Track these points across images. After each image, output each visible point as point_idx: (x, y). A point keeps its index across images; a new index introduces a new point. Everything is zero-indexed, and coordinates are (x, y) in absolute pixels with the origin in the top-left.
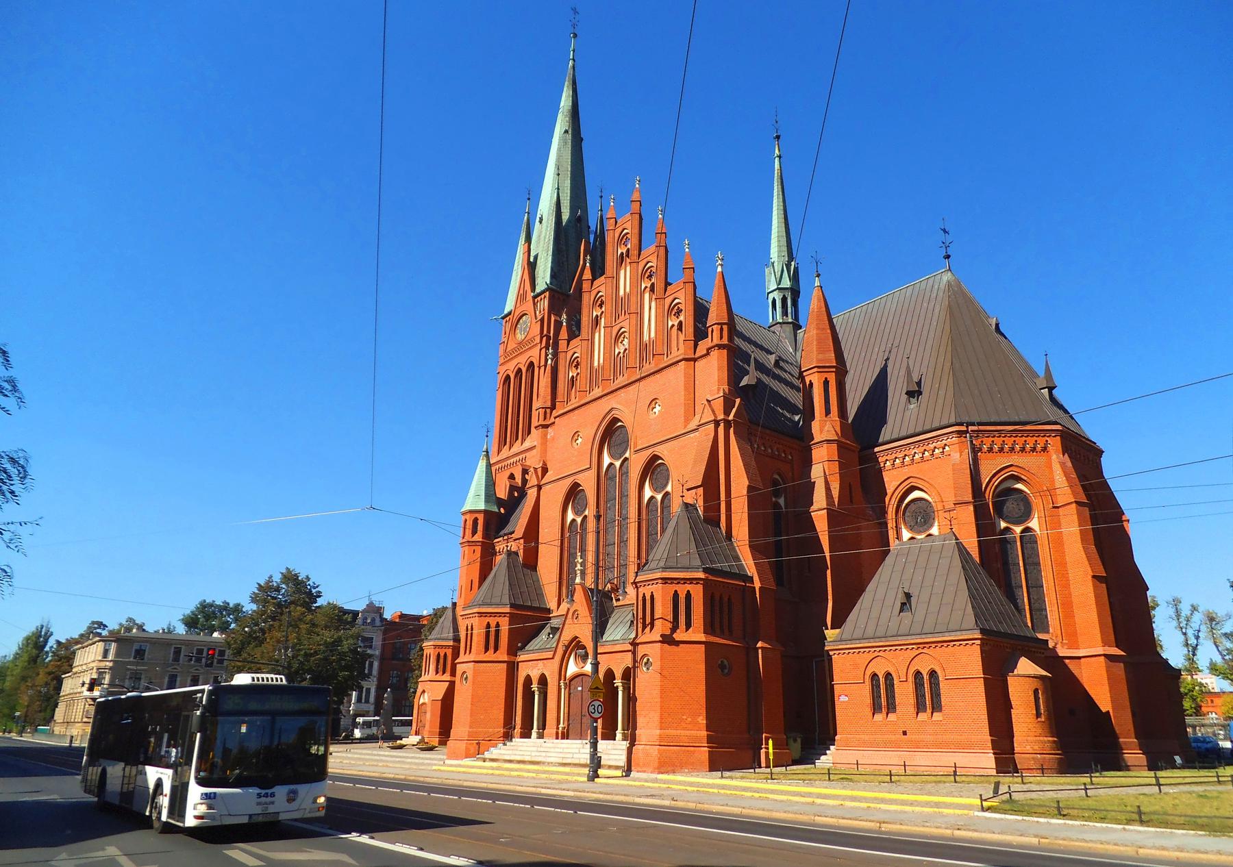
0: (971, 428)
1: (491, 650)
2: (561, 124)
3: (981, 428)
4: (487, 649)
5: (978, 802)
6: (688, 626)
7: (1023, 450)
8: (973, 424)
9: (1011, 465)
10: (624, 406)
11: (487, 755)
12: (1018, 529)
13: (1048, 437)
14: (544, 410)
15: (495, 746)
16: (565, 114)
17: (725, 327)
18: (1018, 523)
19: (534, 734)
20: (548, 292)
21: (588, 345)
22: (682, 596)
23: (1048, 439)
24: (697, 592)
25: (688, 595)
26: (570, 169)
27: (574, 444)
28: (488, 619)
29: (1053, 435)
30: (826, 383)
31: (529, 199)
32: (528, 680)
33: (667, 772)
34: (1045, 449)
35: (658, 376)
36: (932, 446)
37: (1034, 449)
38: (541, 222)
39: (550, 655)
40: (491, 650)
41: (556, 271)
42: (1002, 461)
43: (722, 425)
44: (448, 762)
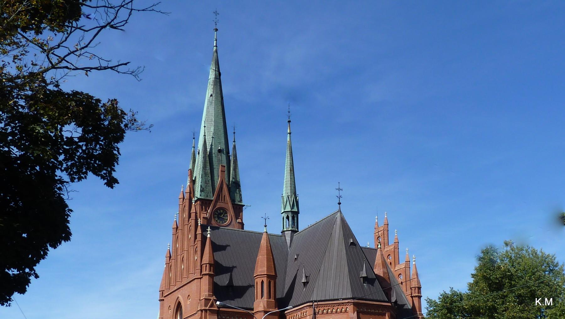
0: (316, 303)
2: (210, 90)
3: (319, 303)
7: (336, 312)
8: (315, 301)
10: (181, 296)
13: (348, 305)
14: (162, 292)
16: (211, 84)
17: (208, 265)
21: (175, 262)
23: (347, 306)
26: (213, 120)
27: (170, 311)
29: (350, 304)
30: (262, 282)
31: (194, 138)
35: (190, 284)
36: (303, 311)
37: (341, 312)
38: (199, 154)
41: (204, 187)
43: (204, 312)
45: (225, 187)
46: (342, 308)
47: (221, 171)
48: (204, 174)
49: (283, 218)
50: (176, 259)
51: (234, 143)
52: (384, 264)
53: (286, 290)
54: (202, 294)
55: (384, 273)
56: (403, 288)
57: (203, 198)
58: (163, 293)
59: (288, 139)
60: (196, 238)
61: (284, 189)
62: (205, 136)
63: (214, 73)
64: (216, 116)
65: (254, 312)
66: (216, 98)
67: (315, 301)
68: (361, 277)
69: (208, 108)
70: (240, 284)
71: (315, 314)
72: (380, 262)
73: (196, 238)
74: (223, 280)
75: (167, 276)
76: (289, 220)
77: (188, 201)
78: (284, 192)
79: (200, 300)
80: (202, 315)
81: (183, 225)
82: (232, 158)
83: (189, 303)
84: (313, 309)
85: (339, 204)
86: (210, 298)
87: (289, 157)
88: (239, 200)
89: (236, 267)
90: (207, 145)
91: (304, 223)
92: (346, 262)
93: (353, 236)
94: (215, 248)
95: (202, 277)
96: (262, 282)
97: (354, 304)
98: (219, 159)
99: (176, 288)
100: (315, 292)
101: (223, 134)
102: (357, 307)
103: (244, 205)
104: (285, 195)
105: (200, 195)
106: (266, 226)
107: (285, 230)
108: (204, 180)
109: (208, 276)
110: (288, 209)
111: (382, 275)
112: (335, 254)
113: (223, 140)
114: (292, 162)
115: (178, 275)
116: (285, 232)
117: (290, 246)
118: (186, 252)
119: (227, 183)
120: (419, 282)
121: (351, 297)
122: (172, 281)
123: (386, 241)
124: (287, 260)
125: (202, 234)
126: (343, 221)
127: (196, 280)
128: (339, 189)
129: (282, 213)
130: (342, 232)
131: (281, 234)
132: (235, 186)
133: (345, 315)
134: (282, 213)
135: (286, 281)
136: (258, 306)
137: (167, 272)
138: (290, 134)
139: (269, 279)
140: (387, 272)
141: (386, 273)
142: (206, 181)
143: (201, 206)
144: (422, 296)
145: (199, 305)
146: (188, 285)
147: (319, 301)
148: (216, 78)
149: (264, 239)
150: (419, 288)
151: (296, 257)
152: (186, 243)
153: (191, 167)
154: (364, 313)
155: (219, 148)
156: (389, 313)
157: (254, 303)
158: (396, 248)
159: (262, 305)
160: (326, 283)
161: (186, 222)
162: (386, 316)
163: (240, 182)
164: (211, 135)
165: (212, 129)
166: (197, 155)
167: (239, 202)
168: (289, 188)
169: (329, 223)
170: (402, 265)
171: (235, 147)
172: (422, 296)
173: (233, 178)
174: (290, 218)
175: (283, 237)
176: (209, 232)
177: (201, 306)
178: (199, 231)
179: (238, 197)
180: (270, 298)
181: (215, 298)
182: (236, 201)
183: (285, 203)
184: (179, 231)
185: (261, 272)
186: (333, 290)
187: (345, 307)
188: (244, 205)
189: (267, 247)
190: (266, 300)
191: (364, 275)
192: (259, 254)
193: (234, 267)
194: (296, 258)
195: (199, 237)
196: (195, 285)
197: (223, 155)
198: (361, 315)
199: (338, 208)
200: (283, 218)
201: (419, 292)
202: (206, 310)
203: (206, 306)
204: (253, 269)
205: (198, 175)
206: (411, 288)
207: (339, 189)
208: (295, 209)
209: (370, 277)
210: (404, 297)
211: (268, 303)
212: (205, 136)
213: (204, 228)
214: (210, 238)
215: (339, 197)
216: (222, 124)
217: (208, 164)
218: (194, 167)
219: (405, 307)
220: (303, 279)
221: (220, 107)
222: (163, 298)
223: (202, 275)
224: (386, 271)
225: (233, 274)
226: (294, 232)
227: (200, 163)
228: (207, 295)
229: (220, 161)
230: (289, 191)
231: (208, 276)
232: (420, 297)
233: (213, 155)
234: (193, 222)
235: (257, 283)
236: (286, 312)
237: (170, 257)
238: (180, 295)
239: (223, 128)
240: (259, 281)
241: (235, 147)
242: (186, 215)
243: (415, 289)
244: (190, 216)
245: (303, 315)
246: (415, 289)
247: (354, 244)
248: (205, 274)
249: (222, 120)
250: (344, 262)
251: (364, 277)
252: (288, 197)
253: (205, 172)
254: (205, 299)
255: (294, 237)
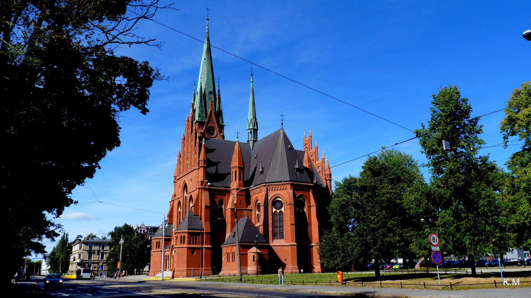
0: (268, 184)
1: (158, 248)
2: (204, 56)
3: (270, 184)
4: (157, 248)
5: (195, 279)
6: (184, 243)
7: (280, 189)
8: (268, 183)
9: (277, 194)
10: (186, 179)
11: (157, 276)
12: (278, 211)
15: (159, 273)
17: (203, 161)
18: (278, 210)
19: (167, 270)
20: (197, 123)
22: (183, 236)
24: (186, 235)
25: (184, 236)
28: (157, 240)
30: (236, 171)
31: (194, 85)
32: (166, 255)
33: (177, 278)
34: (286, 189)
35: (192, 172)
38: (197, 94)
39: (169, 249)
40: (158, 248)
42: (275, 193)
43: (200, 189)
44: (149, 278)
45: (213, 114)
46: (284, 187)
47: (211, 104)
48: (201, 106)
49: (248, 133)
50: (184, 158)
51: (218, 88)
52: (309, 161)
53: (250, 176)
54: (200, 178)
55: (309, 166)
56: (321, 175)
57: (200, 120)
58: (176, 178)
59: (251, 85)
60: (195, 145)
61: (249, 115)
62: (201, 83)
63: (207, 45)
64: (208, 71)
65: (231, 189)
66: (207, 61)
67: (268, 183)
68: (295, 168)
69: (203, 66)
70: (223, 172)
71: (267, 190)
72: (307, 159)
73: (195, 145)
74: (212, 170)
75: (178, 168)
76: (251, 134)
77: (191, 122)
78: (249, 117)
79: (198, 182)
80: (199, 191)
81: (188, 137)
82: (217, 97)
83: (191, 184)
84: (266, 188)
85: (282, 124)
86: (204, 181)
87: (252, 96)
88: (222, 122)
89: (220, 162)
90: (202, 89)
91: (261, 135)
92: (286, 160)
93: (290, 144)
94: (207, 151)
95: (199, 168)
96: (236, 171)
97: (291, 184)
98: (210, 97)
99: (183, 175)
100: (267, 177)
101: (212, 82)
102: (293, 187)
103: (225, 125)
104: (249, 119)
105: (198, 119)
106: (238, 138)
107: (249, 140)
108: (201, 110)
109: (203, 168)
110: (251, 127)
111: (308, 167)
112: (280, 154)
113: (212, 86)
114: (253, 99)
115: (185, 167)
116: (250, 141)
117: (252, 150)
118: (189, 153)
119: (214, 111)
120: (330, 171)
121: (289, 180)
122: (181, 170)
123: (310, 147)
124: (250, 158)
125: (199, 142)
126: (284, 135)
127: (196, 170)
128: (282, 115)
129: (248, 130)
130: (284, 141)
131: (247, 142)
132: (219, 114)
133: (286, 191)
134: (248, 130)
135: (250, 171)
136: (233, 186)
137: (178, 165)
138: (252, 82)
139: (240, 170)
140: (311, 165)
141: (310, 166)
142: (202, 110)
143: (199, 125)
144: (332, 180)
145: (198, 185)
146: (191, 173)
147: (270, 183)
148: (208, 48)
149: (237, 145)
150: (330, 175)
151: (256, 156)
152: (189, 148)
153: (192, 102)
154: (298, 190)
155: (210, 91)
156: (312, 190)
157: (231, 184)
158: (317, 151)
159: (235, 185)
160: (274, 172)
161: (190, 135)
162: (310, 191)
163: (222, 111)
164: (205, 82)
165: (205, 79)
166: (197, 95)
167: (222, 123)
168: (252, 115)
169: (276, 135)
170: (320, 161)
171: (219, 90)
172: (332, 180)
173: (218, 109)
174: (253, 133)
175: (248, 144)
176: (203, 141)
177: (199, 185)
178: (198, 140)
179: (221, 120)
180: (240, 181)
181: (207, 181)
182: (220, 122)
183: (249, 124)
184: (186, 141)
185: (235, 165)
186: (278, 176)
187: (285, 186)
188: (225, 125)
189: (239, 150)
190: (238, 182)
191: (297, 167)
192: (234, 154)
193: (219, 162)
194: (256, 157)
195: (198, 144)
196: (195, 173)
197: (212, 95)
198: (295, 191)
199: (282, 127)
200: (248, 133)
201: (330, 177)
202: (202, 188)
203: (202, 185)
204: (230, 163)
205: (197, 107)
206: (325, 175)
207: (282, 115)
208: (256, 128)
209: (301, 168)
210: (321, 180)
211: (240, 185)
212: (201, 83)
213: (201, 139)
214: (204, 145)
215: (282, 120)
216: (212, 76)
217: (203, 101)
218: (195, 102)
219: (322, 187)
220: (260, 169)
221: (210, 66)
222: (176, 181)
223: (200, 167)
224: (310, 165)
225: (218, 166)
226: (254, 141)
227: (198, 100)
228: (203, 179)
229: (210, 98)
230: (252, 117)
231: (203, 168)
232: (331, 180)
233: (206, 95)
234: (194, 135)
235: (232, 172)
236: (250, 189)
237: (180, 156)
238: (187, 179)
239: (212, 79)
240: (233, 170)
241: (219, 90)
242: (190, 131)
243: (328, 175)
244: (192, 132)
245: (260, 191)
246: (328, 175)
247: (291, 148)
248: (201, 167)
249: (211, 74)
250: (285, 160)
251: (297, 168)
252: (251, 120)
253: (201, 105)
254: (201, 182)
255: (255, 144)
